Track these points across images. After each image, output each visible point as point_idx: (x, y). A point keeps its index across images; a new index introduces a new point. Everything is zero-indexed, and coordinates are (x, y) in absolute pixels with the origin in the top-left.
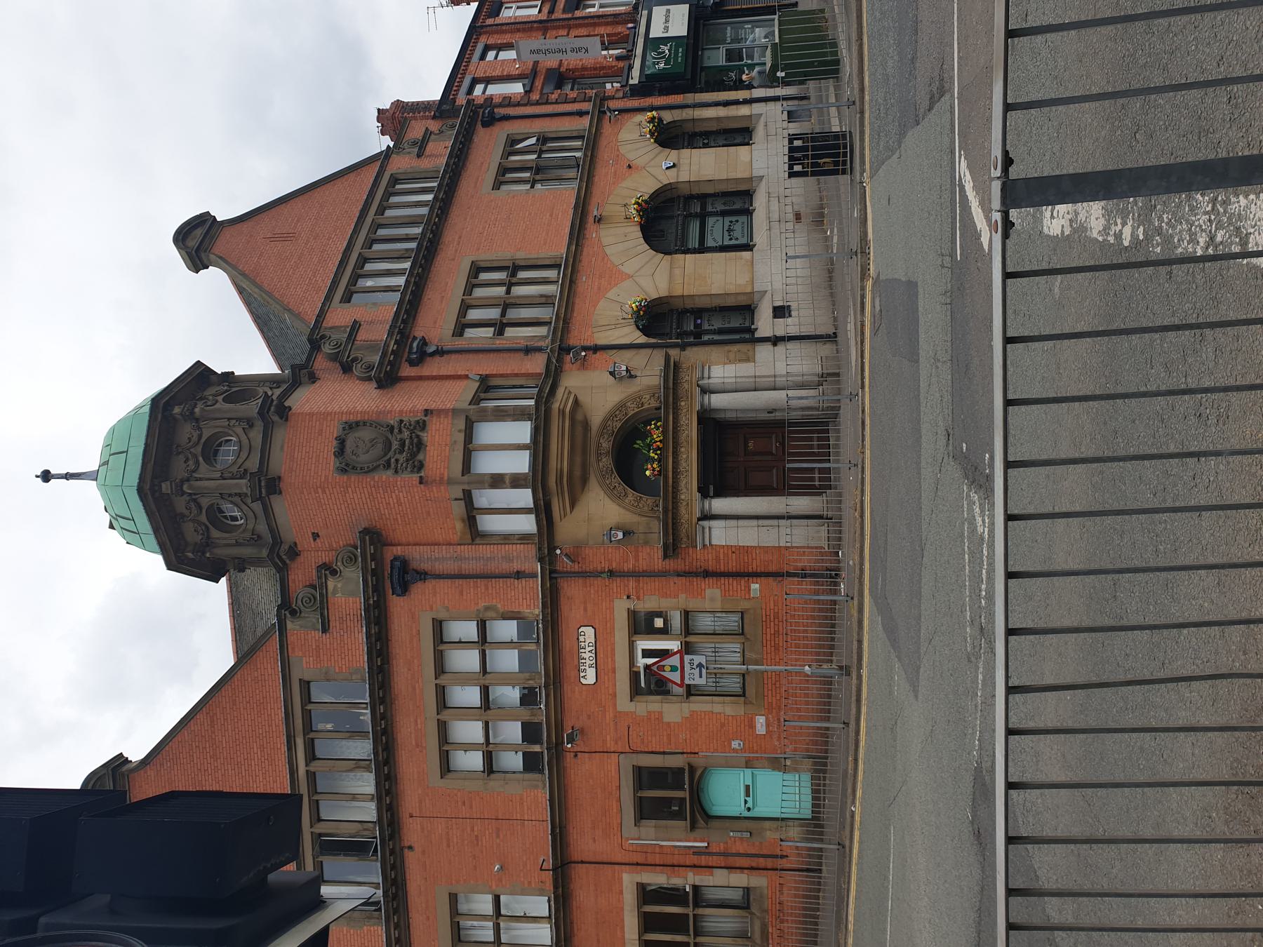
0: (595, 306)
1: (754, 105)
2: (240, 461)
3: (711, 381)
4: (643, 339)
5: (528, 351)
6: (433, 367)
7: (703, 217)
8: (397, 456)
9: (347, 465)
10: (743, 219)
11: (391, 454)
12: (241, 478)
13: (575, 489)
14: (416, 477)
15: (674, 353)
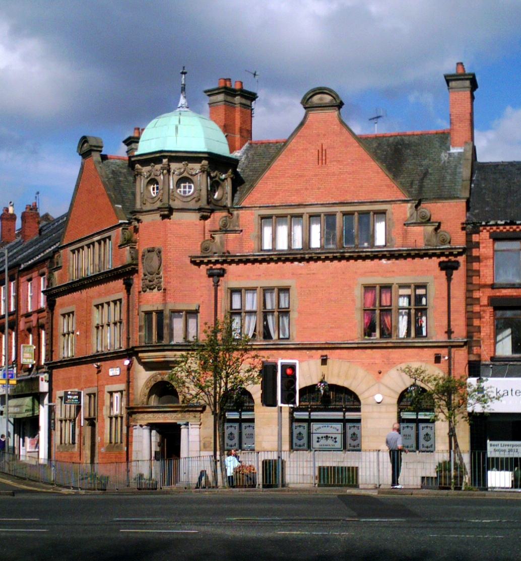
10: (339, 445)
14: (141, 289)
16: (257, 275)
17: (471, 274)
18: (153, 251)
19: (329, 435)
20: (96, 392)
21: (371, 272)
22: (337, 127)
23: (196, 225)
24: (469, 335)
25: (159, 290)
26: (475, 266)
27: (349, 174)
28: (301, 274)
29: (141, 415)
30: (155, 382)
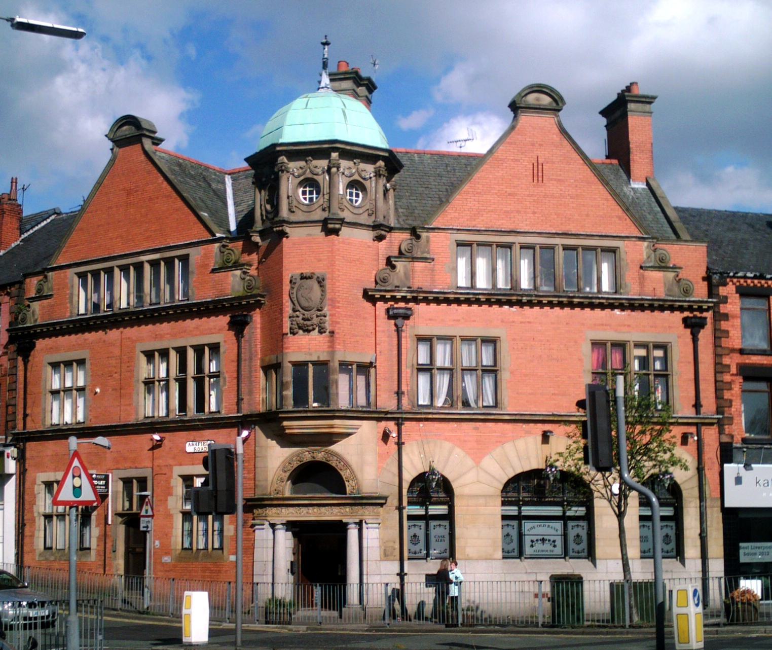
0: (446, 439)
1: (699, 562)
5: (399, 393)
7: (564, 518)
8: (301, 317)
9: (295, 283)
10: (559, 550)
15: (393, 501)
16: (454, 320)
17: (719, 335)
18: (310, 278)
19: (545, 537)
20: (147, 473)
21: (602, 325)
22: (556, 136)
23: (369, 247)
24: (719, 410)
25: (320, 332)
26: (724, 325)
27: (571, 198)
28: (513, 322)
29: (274, 510)
30: (299, 463)
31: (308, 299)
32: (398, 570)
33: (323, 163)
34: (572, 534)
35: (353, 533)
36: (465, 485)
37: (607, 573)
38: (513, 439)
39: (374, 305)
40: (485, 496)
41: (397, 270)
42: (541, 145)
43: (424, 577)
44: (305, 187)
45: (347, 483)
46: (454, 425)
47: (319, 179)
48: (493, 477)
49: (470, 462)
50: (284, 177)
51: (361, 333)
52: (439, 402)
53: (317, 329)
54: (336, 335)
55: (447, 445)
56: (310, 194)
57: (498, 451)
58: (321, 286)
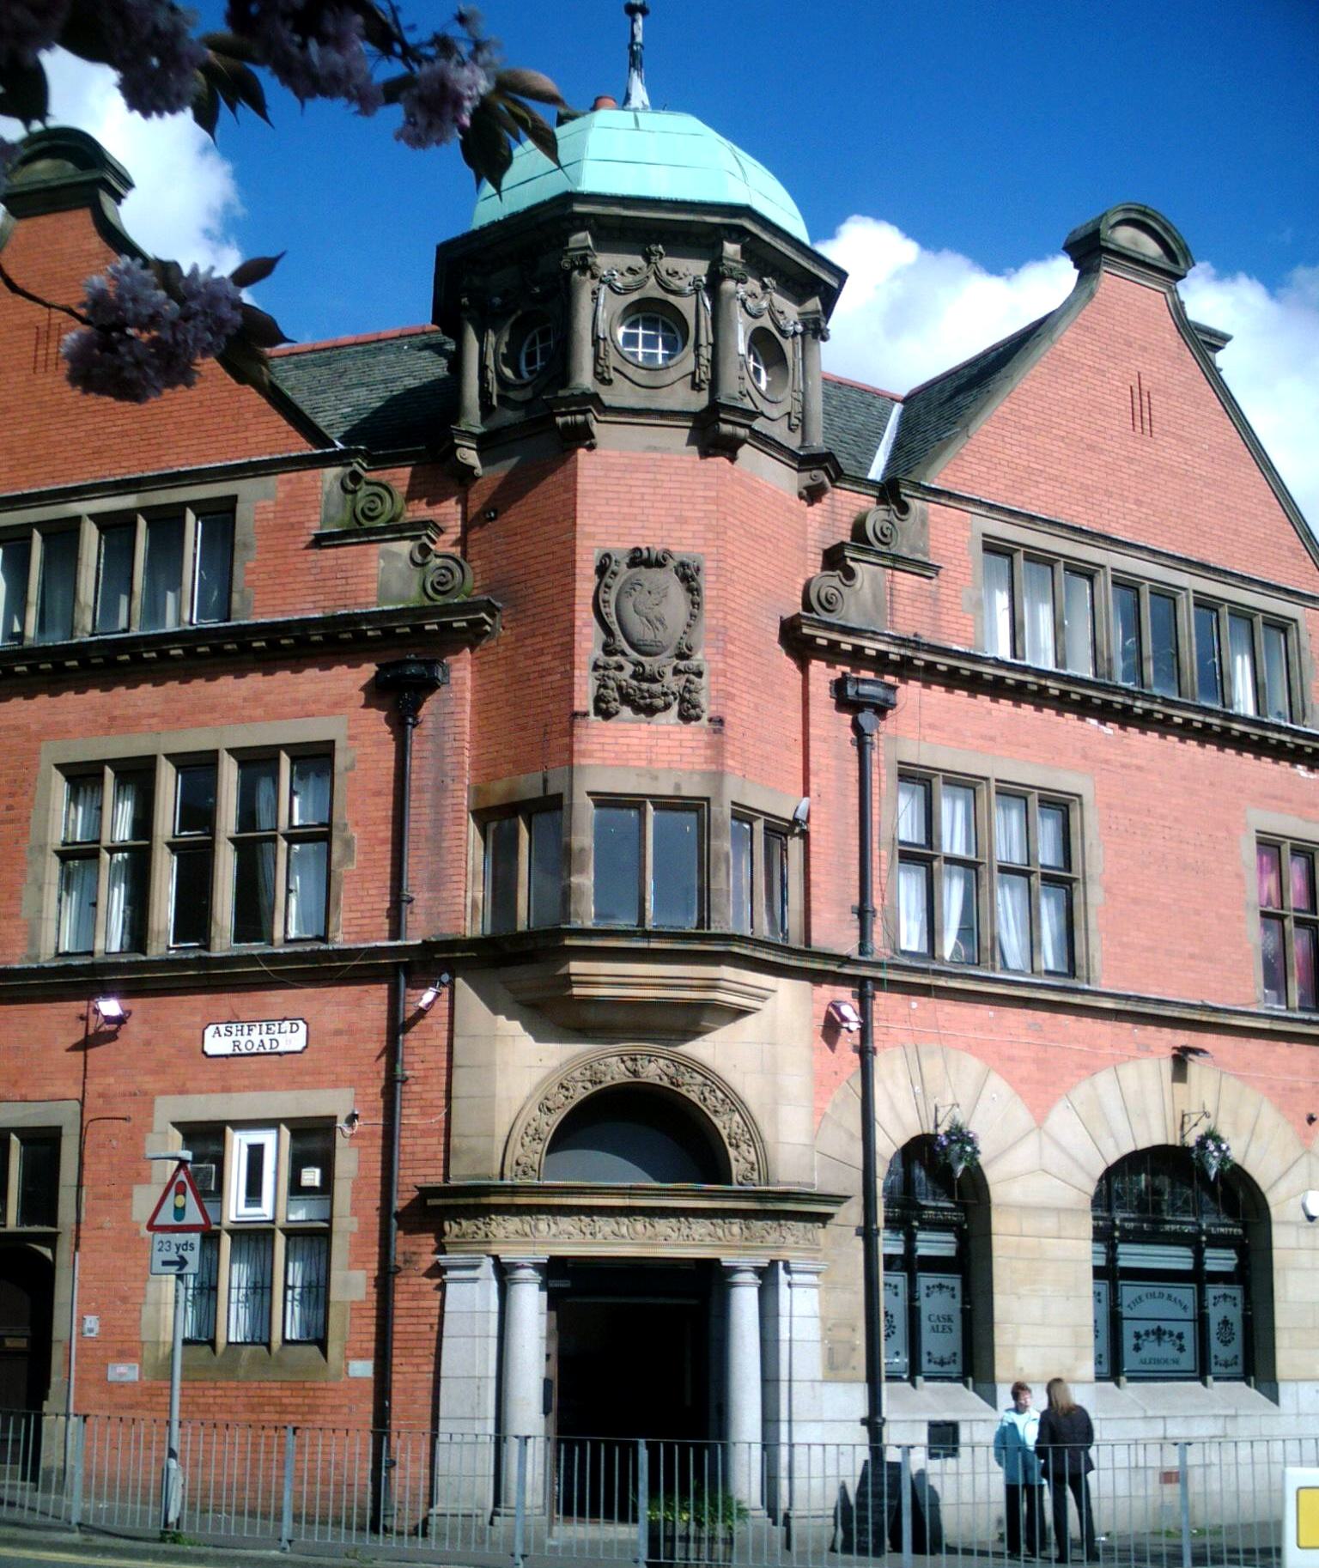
0: (969, 1049)
2: (629, 370)
3: (784, 1291)
4: (888, 1144)
6: (832, 726)
7: (1198, 1277)
8: (629, 669)
10: (1188, 1361)
11: (635, 655)
12: (596, 373)
13: (558, 1014)
15: (852, 1213)
16: (983, 737)
18: (659, 564)
19: (1165, 1326)
21: (1275, 797)
23: (790, 510)
25: (685, 717)
27: (1207, 485)
28: (1107, 762)
30: (592, 1089)
31: (656, 622)
32: (862, 1410)
33: (697, 268)
34: (1215, 1314)
35: (745, 1301)
36: (1013, 1178)
37: (1298, 1415)
38: (1115, 1063)
39: (804, 668)
40: (1058, 1211)
41: (858, 583)
42: (1144, 349)
43: (925, 1429)
44: (634, 325)
45: (732, 1152)
46: (986, 1012)
47: (686, 305)
48: (1074, 1160)
49: (1022, 1116)
50: (586, 287)
51: (765, 740)
52: (949, 943)
53: (675, 708)
54: (728, 731)
55: (973, 1065)
56: (645, 345)
57: (1082, 1091)
58: (690, 590)
